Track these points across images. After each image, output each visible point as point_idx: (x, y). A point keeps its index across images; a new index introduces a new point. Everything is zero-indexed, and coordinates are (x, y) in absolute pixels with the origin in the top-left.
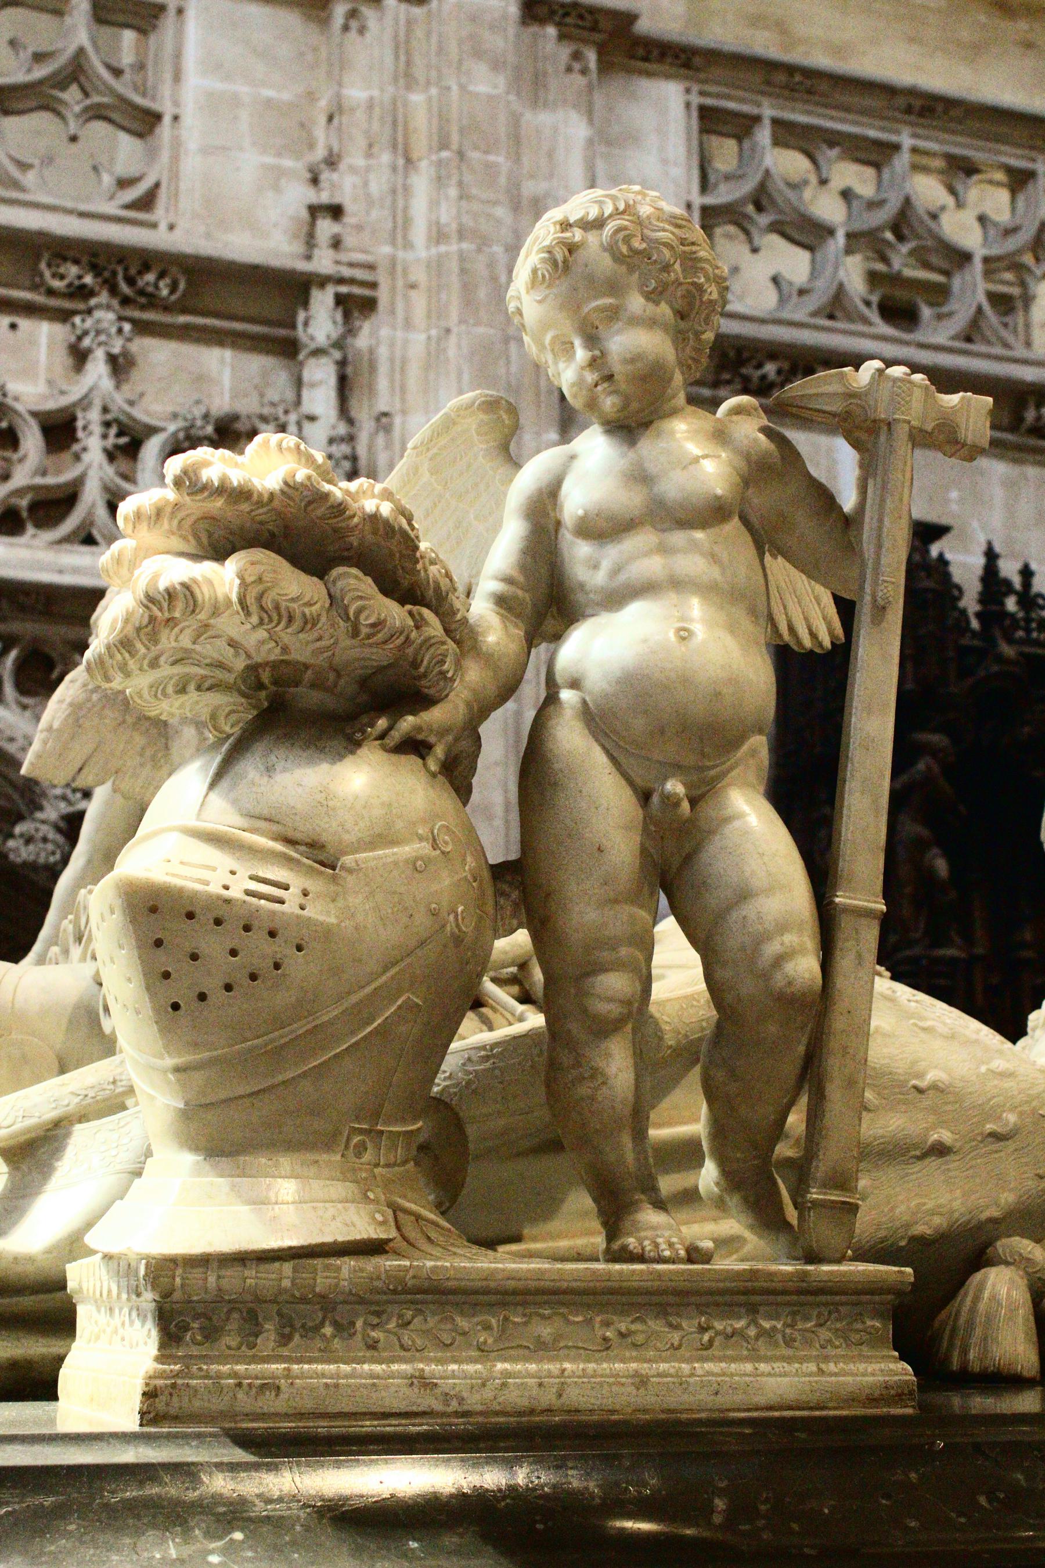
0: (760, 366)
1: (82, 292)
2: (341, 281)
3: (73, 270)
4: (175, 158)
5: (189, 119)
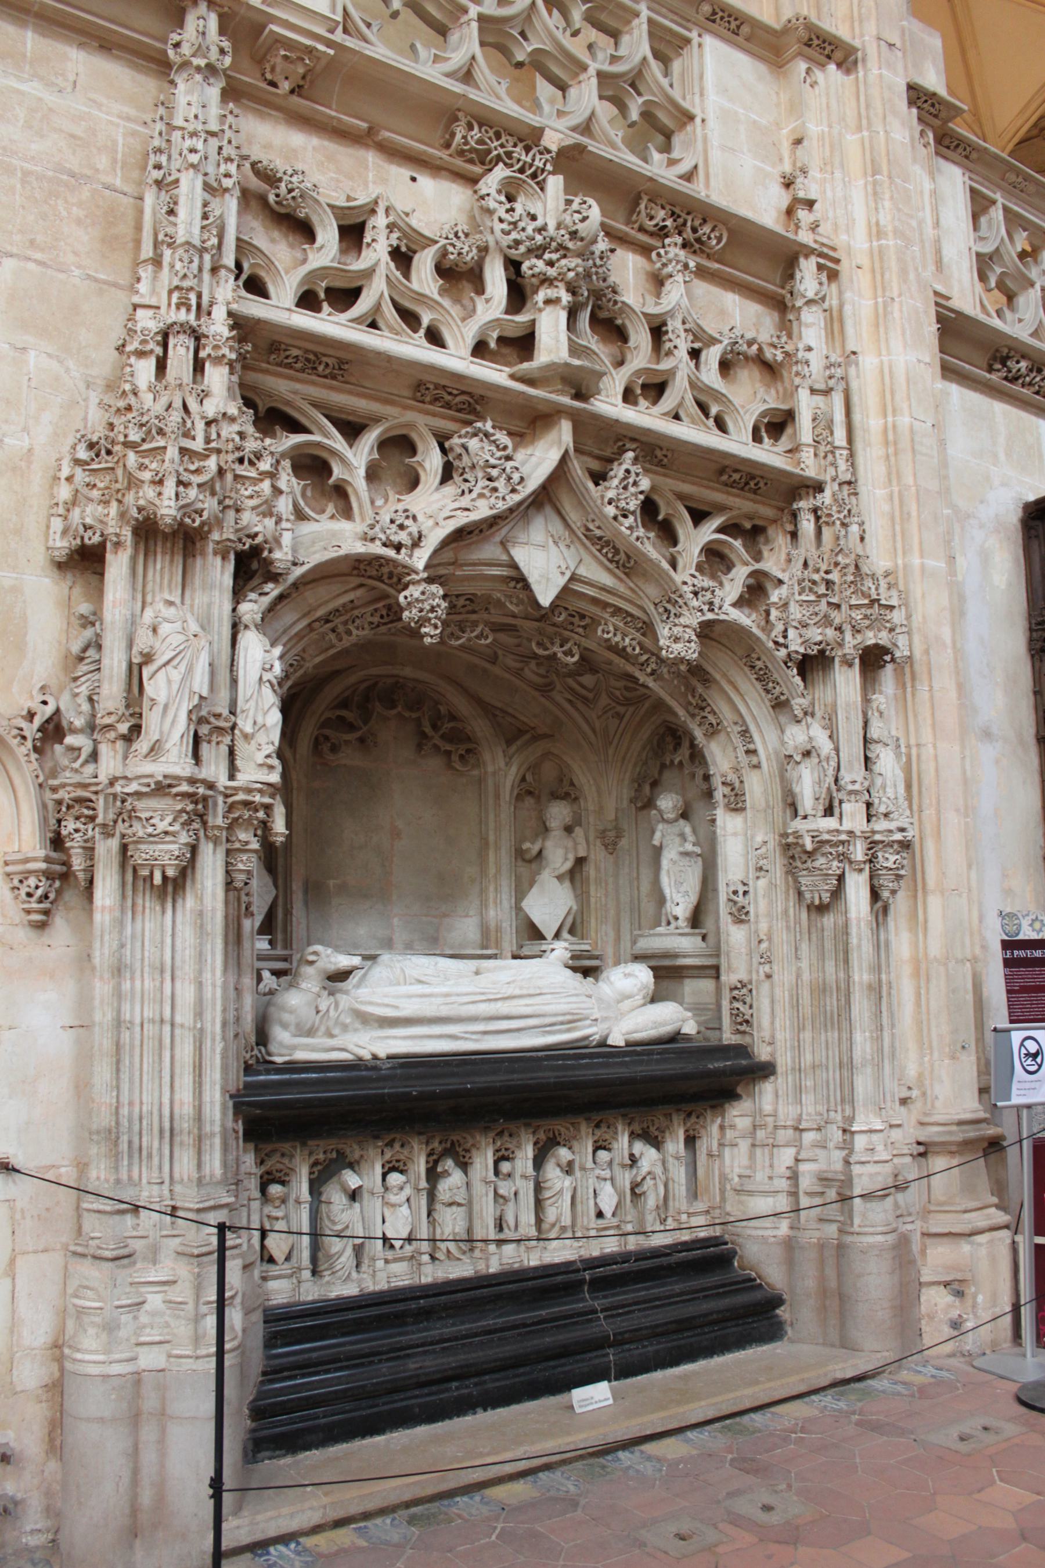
0: (1018, 362)
1: (662, 233)
2: (821, 255)
3: (662, 214)
4: (706, 151)
5: (711, 123)
